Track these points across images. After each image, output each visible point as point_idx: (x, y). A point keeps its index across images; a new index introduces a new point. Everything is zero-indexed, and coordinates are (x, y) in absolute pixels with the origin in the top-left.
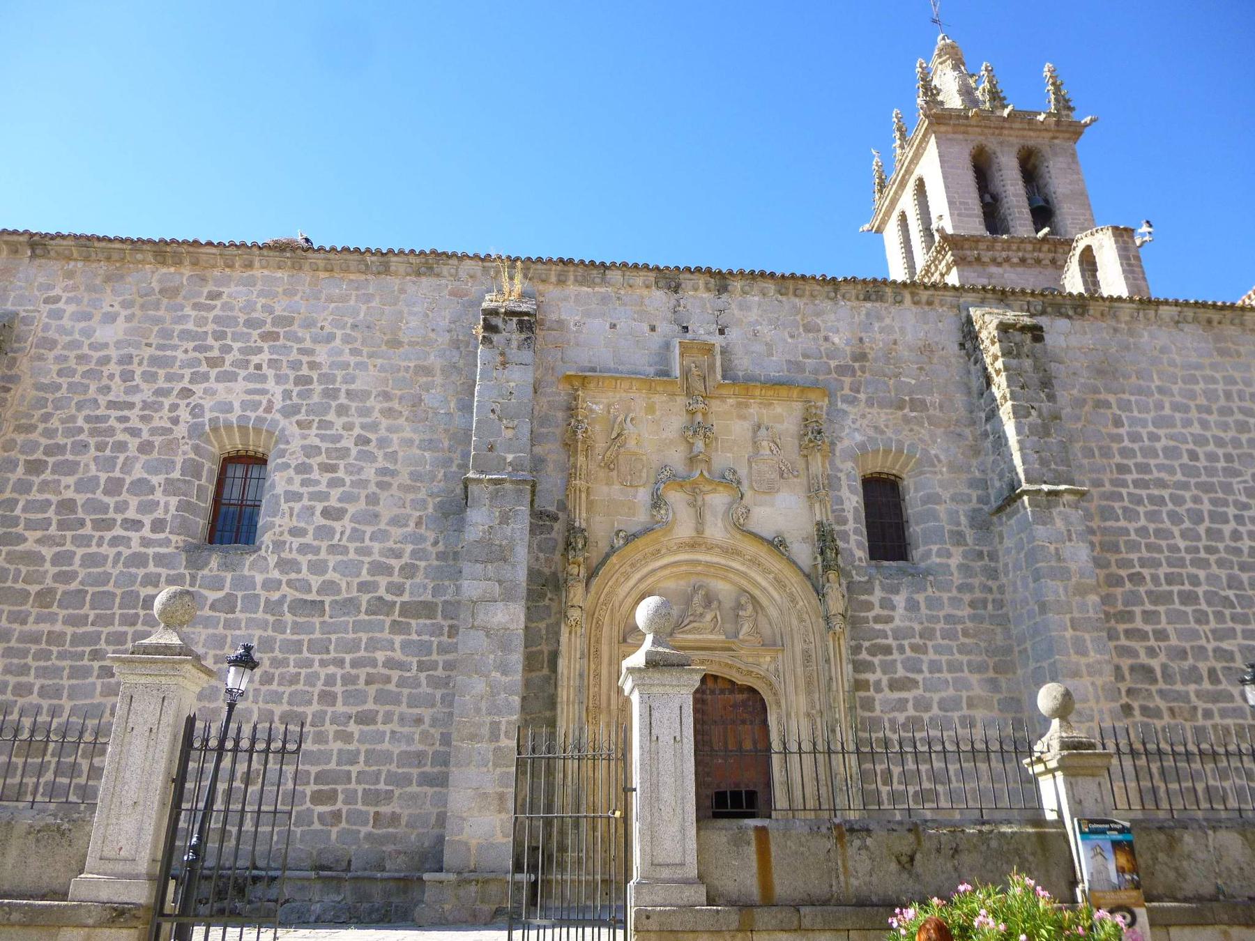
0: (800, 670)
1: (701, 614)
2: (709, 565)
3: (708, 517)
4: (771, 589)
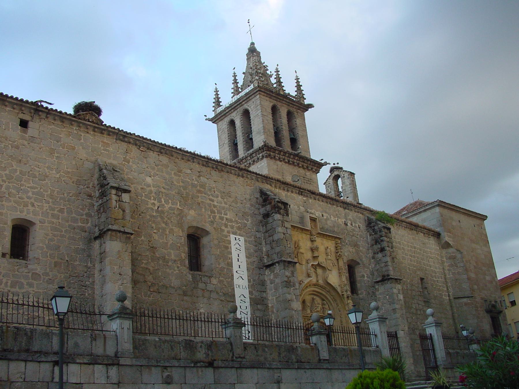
3: (319, 277)
4: (331, 301)
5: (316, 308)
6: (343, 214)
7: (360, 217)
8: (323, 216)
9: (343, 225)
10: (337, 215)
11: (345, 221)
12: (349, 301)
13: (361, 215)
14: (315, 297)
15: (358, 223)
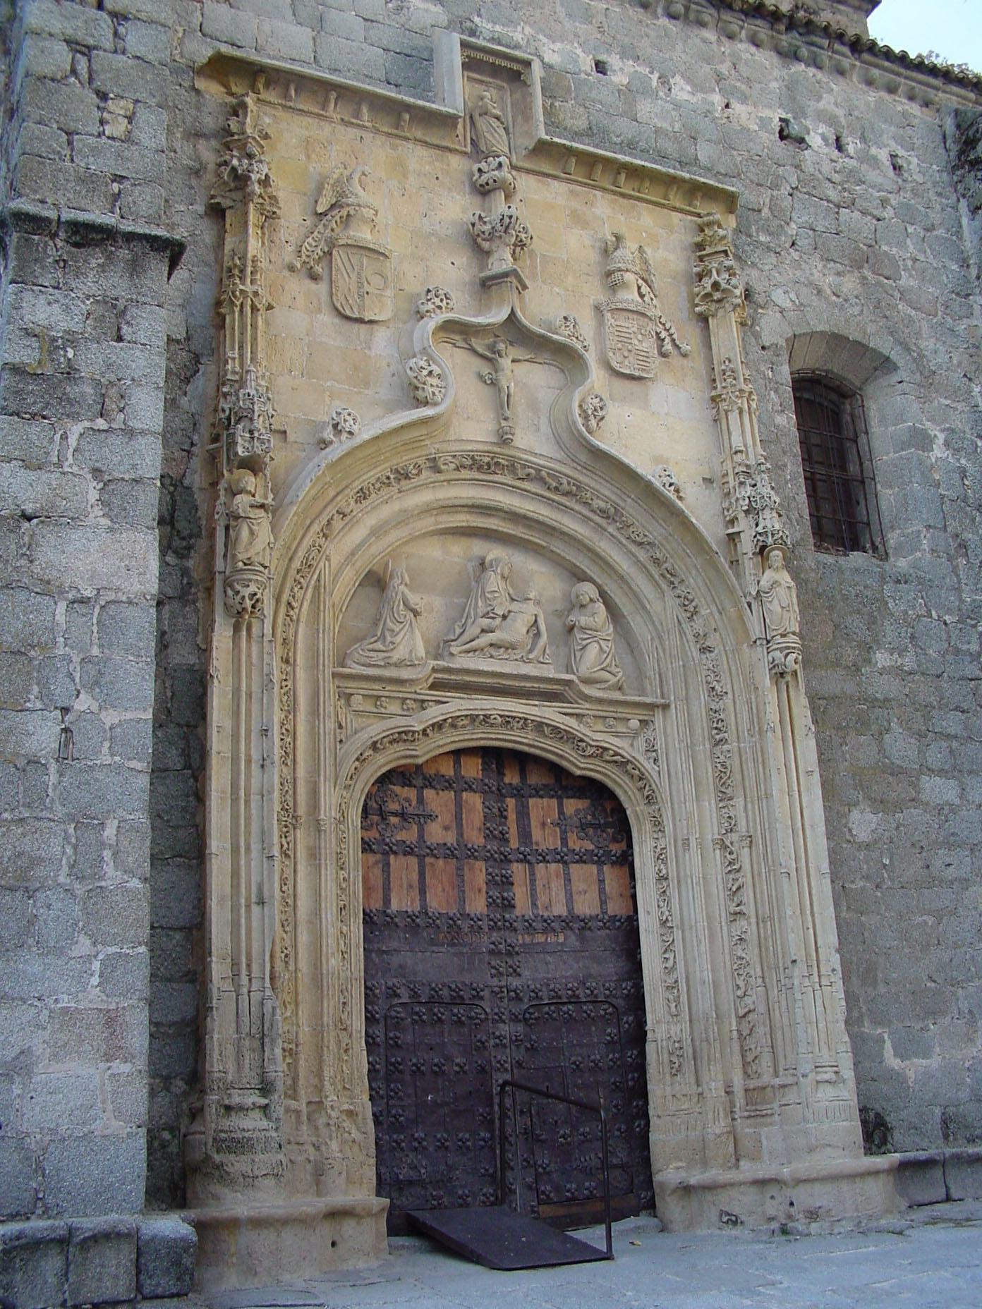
0: (703, 748)
1: (504, 617)
2: (515, 517)
5: (485, 622)
6: (774, 85)
7: (905, 115)
8: (600, 67)
9: (770, 138)
10: (720, 78)
11: (781, 120)
12: (768, 577)
13: (915, 109)
14: (494, 552)
15: (892, 143)
